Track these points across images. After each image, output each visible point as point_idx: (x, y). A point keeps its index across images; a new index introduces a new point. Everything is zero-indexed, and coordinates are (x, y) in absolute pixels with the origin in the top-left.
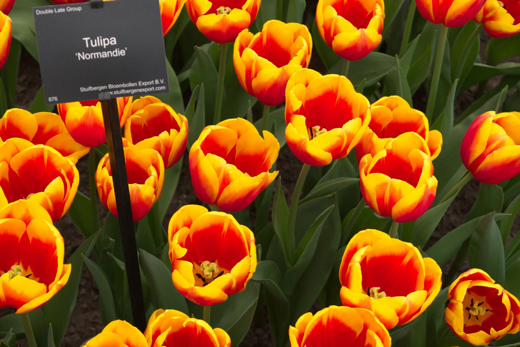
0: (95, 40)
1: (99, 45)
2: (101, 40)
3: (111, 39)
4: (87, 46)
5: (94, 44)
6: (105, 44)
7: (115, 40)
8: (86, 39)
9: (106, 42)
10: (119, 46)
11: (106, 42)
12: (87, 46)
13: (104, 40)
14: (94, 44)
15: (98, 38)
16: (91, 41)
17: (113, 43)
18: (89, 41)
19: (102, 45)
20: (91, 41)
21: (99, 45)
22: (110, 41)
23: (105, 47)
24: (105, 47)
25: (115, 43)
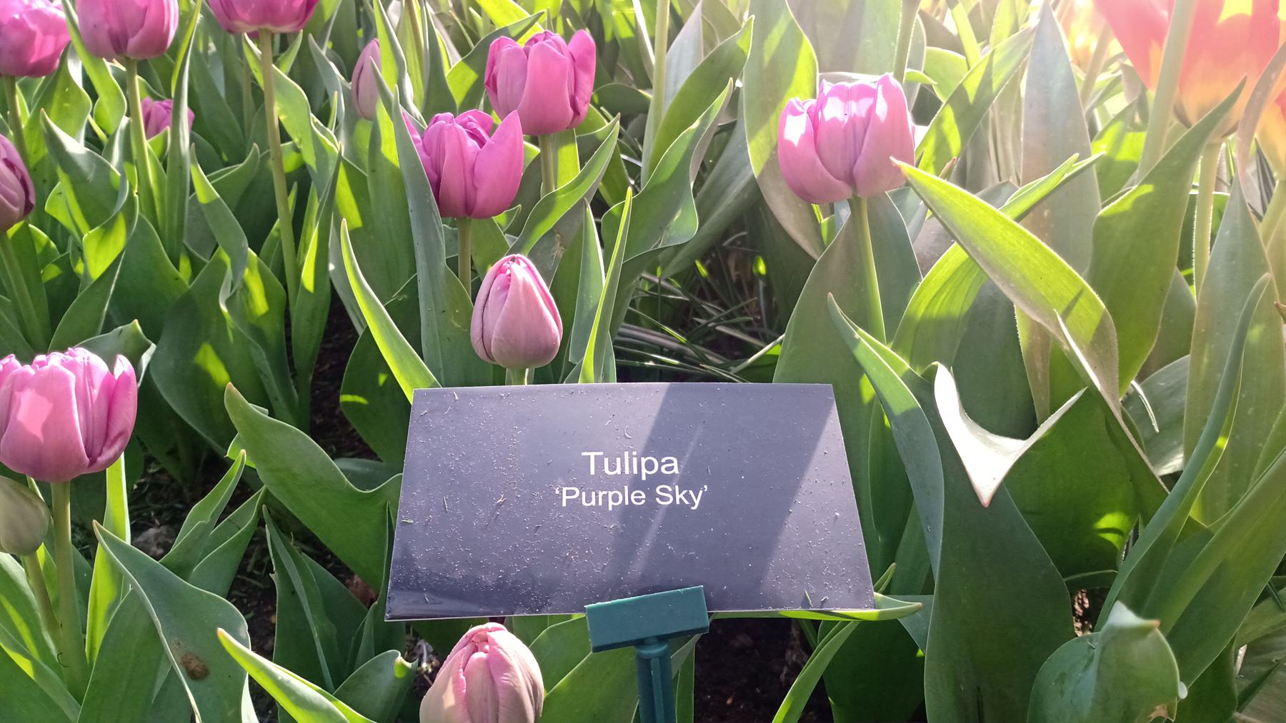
0: (618, 460)
1: (627, 472)
2: (635, 460)
3: (663, 460)
4: (592, 472)
5: (612, 468)
6: (644, 471)
7: (675, 464)
8: (592, 455)
9: (650, 466)
10: (686, 482)
11: (650, 466)
12: (592, 472)
13: (644, 460)
14: (612, 468)
15: (626, 454)
16: (606, 460)
17: (667, 469)
18: (599, 461)
19: (635, 472)
20: (606, 460)
21: (627, 472)
22: (661, 465)
23: (644, 478)
24: (644, 478)
25: (676, 470)
